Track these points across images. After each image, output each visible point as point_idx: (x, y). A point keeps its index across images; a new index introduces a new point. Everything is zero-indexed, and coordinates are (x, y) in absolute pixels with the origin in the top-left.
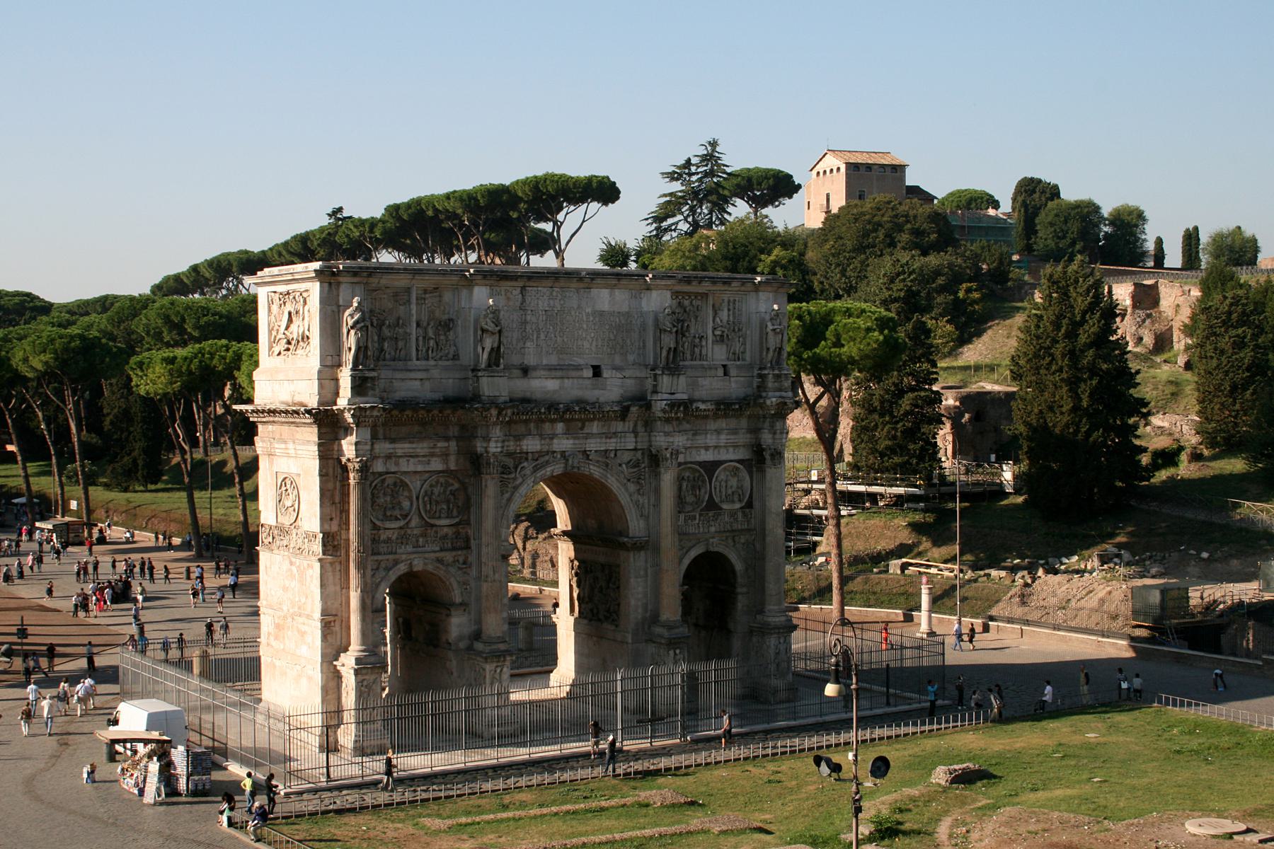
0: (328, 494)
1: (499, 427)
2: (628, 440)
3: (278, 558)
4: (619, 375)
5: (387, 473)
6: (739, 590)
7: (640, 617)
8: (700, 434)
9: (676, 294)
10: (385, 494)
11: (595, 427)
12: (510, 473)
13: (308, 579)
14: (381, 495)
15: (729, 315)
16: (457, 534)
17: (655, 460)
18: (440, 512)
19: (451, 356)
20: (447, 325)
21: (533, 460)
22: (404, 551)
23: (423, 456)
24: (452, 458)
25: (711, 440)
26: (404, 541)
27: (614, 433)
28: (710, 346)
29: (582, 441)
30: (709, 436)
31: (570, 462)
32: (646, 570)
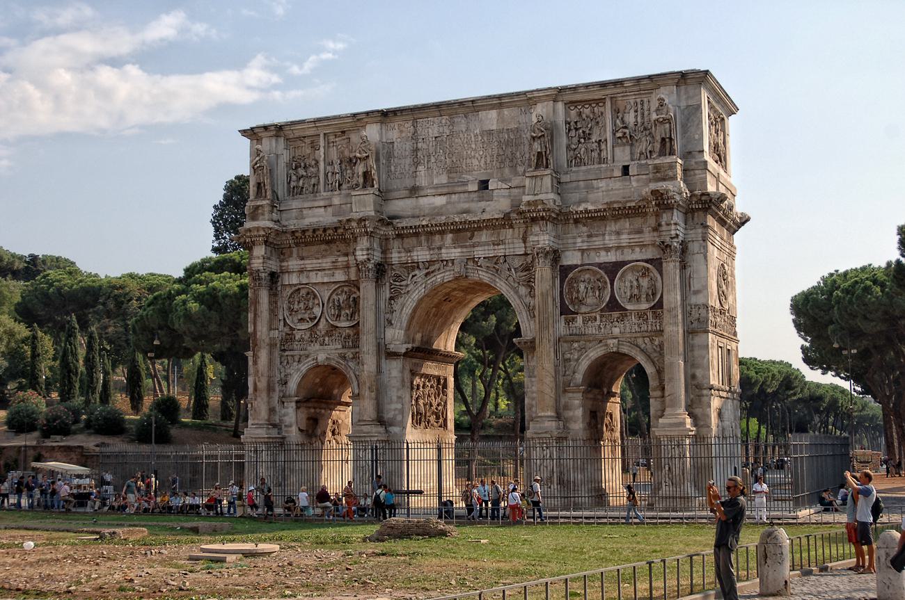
2: (517, 245)
4: (505, 186)
5: (300, 284)
9: (570, 104)
10: (299, 302)
11: (484, 236)
14: (296, 303)
25: (610, 240)
29: (473, 249)
30: (607, 237)
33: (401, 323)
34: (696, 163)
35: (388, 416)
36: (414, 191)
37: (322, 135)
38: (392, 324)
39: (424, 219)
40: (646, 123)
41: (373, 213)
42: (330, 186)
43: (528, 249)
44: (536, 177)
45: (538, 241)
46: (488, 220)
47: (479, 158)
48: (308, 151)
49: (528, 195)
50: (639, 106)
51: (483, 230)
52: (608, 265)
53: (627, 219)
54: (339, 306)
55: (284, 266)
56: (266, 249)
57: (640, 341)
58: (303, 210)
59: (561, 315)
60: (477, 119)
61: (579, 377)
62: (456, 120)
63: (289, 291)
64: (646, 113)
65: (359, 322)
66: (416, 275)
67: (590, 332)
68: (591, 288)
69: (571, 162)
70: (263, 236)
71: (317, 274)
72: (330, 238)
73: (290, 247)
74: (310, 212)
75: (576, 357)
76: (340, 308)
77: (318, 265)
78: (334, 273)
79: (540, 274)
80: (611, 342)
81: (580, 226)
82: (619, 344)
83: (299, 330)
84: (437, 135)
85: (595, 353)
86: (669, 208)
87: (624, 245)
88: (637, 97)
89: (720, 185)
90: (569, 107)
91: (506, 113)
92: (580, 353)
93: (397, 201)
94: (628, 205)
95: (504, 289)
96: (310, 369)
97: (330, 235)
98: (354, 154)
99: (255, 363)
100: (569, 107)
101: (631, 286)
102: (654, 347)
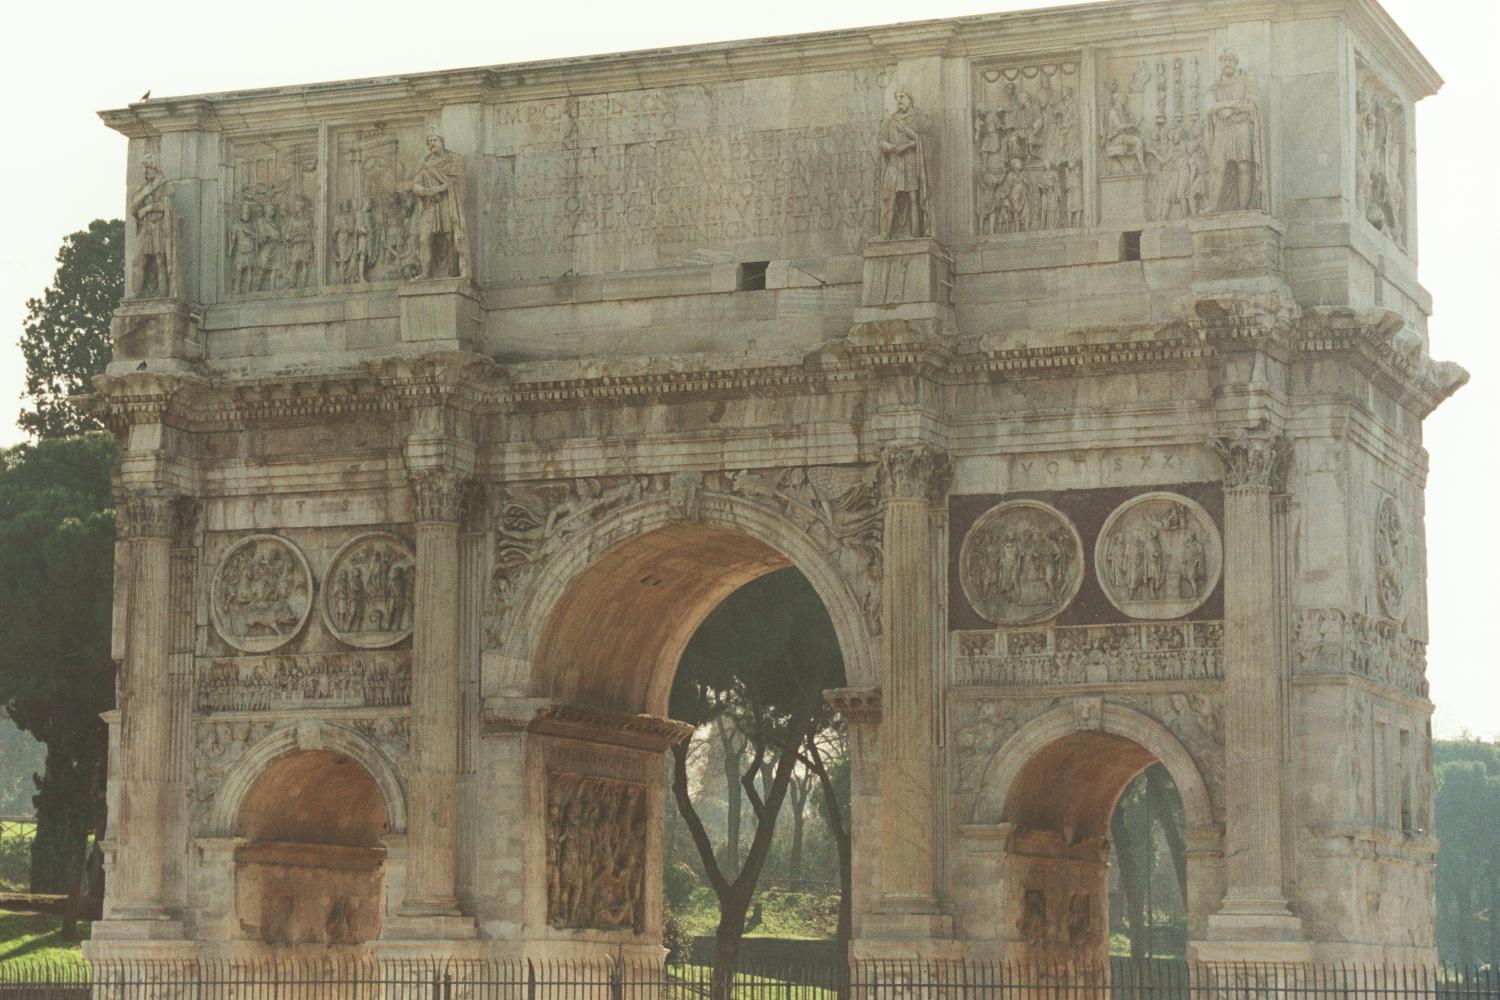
1: (434, 412)
4: (808, 281)
8: (1050, 418)
9: (985, 64)
10: (251, 579)
11: (750, 413)
12: (533, 527)
14: (244, 581)
15: (1162, 103)
21: (595, 497)
23: (335, 493)
25: (1085, 432)
27: (798, 427)
29: (718, 447)
30: (1077, 423)
33: (524, 642)
34: (1319, 229)
35: (483, 889)
36: (567, 287)
37: (322, 134)
38: (499, 645)
39: (591, 365)
40: (1187, 121)
41: (455, 346)
43: (866, 449)
44: (891, 258)
45: (893, 430)
46: (766, 369)
47: (742, 203)
49: (870, 307)
50: (1171, 74)
51: (746, 397)
52: (1079, 498)
53: (1132, 376)
54: (360, 591)
55: (213, 481)
56: (164, 434)
57: (1160, 704)
58: (269, 330)
59: (952, 627)
60: (739, 99)
61: (998, 795)
62: (682, 99)
63: (225, 549)
64: (1189, 93)
65: (411, 636)
66: (566, 514)
67: (1028, 676)
68: (1033, 558)
69: (987, 218)
70: (159, 398)
71: (301, 504)
72: (339, 408)
73: (230, 430)
74: (288, 336)
75: (989, 743)
76: (361, 598)
77: (306, 481)
78: (346, 502)
79: (896, 519)
80: (1085, 704)
81: (1008, 391)
82: (1103, 710)
83: (248, 654)
84: (627, 142)
85: (1042, 733)
86: (1245, 348)
88: (1165, 49)
89: (1386, 287)
90: (983, 74)
91: (814, 83)
92: (1000, 732)
93: (520, 312)
94: (1135, 337)
95: (800, 556)
96: (275, 760)
97: (338, 400)
98: (407, 186)
99: (127, 740)
100: (983, 74)
101: (1141, 556)
102: (1200, 720)
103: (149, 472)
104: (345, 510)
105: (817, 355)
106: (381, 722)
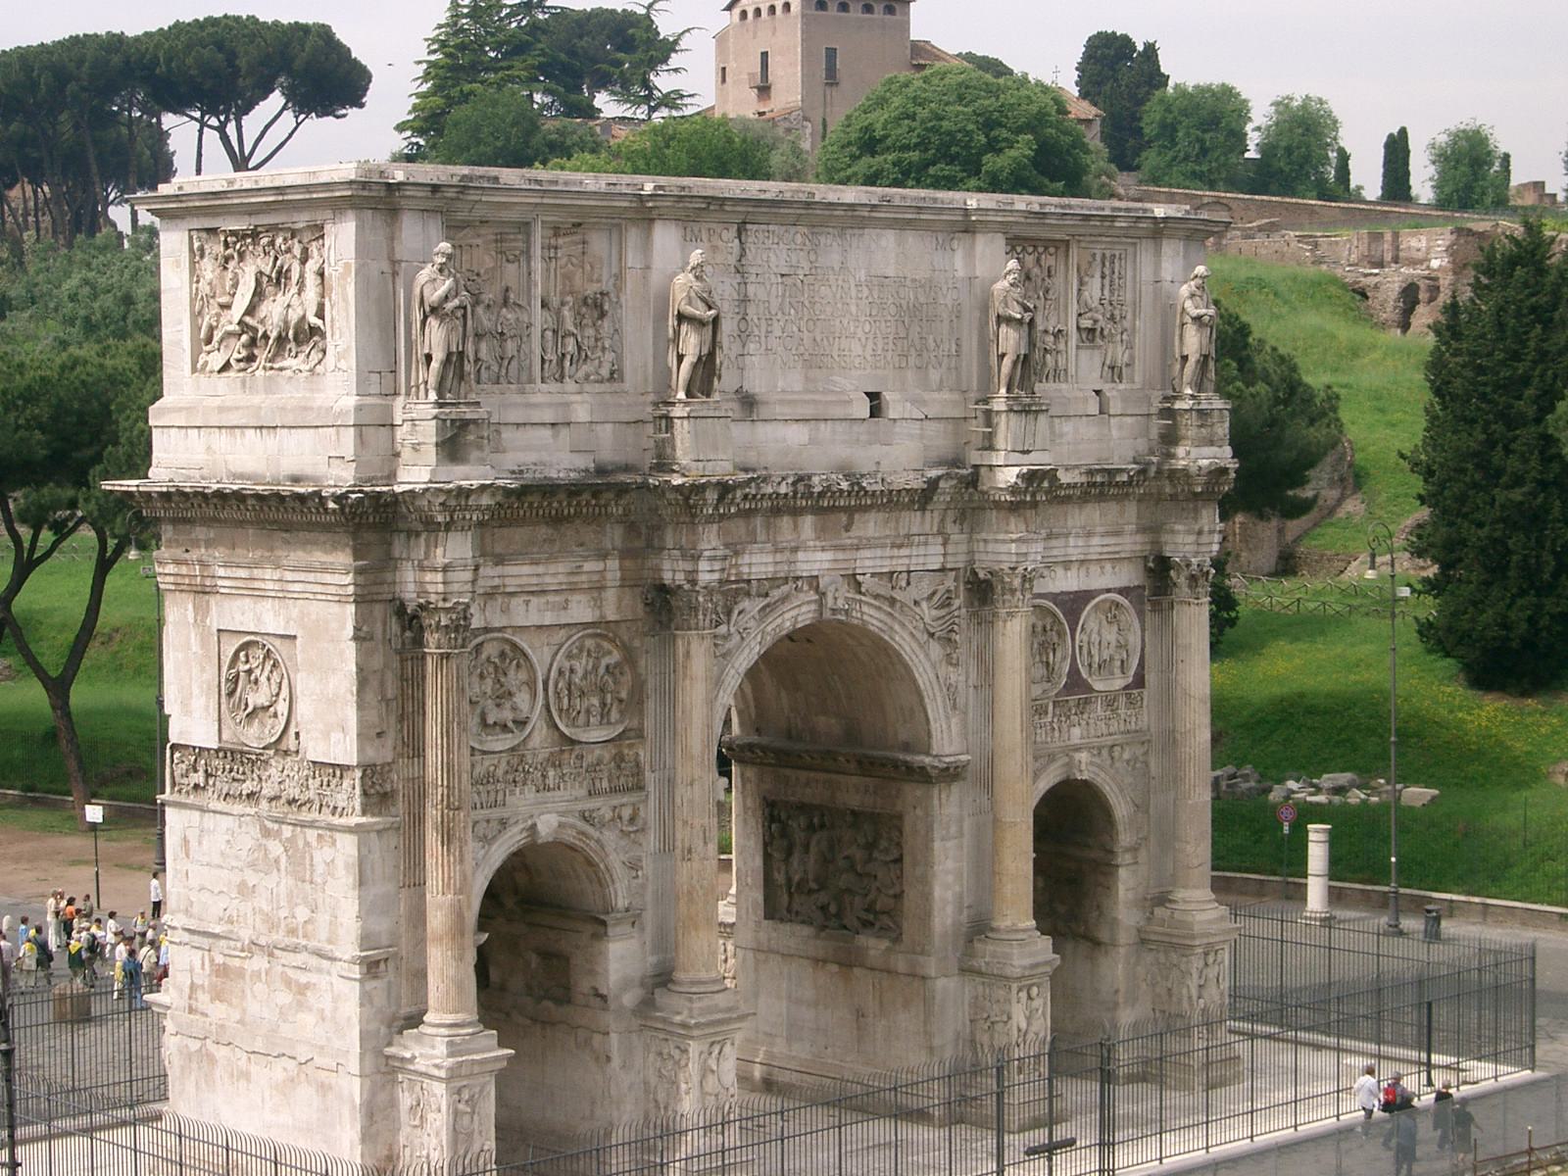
0: (375, 683)
2: (932, 550)
3: (226, 822)
6: (1124, 858)
7: (949, 921)
8: (1057, 536)
11: (870, 525)
13: (320, 868)
16: (619, 759)
17: (982, 590)
18: (588, 712)
19: (605, 372)
20: (596, 307)
21: (759, 596)
22: (522, 801)
24: (610, 595)
25: (1074, 548)
26: (520, 777)
28: (1072, 351)
30: (1072, 541)
31: (830, 596)
32: (961, 820)
42: (546, 366)
43: (949, 558)
48: (489, 263)
58: (502, 428)
62: (822, 239)
71: (527, 603)
77: (534, 580)
78: (567, 601)
83: (484, 753)
87: (1095, 557)
95: (907, 649)
103: (466, 583)
104: (565, 608)
105: (939, 478)
106: (602, 812)
